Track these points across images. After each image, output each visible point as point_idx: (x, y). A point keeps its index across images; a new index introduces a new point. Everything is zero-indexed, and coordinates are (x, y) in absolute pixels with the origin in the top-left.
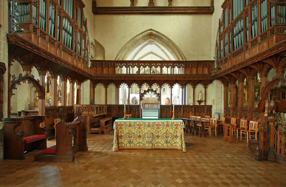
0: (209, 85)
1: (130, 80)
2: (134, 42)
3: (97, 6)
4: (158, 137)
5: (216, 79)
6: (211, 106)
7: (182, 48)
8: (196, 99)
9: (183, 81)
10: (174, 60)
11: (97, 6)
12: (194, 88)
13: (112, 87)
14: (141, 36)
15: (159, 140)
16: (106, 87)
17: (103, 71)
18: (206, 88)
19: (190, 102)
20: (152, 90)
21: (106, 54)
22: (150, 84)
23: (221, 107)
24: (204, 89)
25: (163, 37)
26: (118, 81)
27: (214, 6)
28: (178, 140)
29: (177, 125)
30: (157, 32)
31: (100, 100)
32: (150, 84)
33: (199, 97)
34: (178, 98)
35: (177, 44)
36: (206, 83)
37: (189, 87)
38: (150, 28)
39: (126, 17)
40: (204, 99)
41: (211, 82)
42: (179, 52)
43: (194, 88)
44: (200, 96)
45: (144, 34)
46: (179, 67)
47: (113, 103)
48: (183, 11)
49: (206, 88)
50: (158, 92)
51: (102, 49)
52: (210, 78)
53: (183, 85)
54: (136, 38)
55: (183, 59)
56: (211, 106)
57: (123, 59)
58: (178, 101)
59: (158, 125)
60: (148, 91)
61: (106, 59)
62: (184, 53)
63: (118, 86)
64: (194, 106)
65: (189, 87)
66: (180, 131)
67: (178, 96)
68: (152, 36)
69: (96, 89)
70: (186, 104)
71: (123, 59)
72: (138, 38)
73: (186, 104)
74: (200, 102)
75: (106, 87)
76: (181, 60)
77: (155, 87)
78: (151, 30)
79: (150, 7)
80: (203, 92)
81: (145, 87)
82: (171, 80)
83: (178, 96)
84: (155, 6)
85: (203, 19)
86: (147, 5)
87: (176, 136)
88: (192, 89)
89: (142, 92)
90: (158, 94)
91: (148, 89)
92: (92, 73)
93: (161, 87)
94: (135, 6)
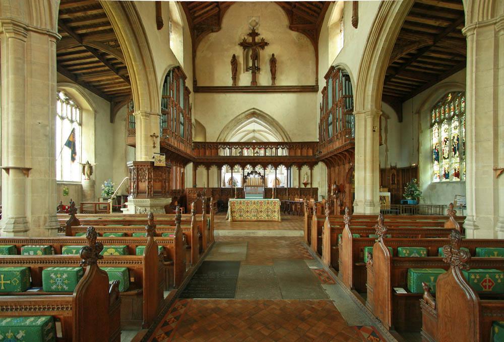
0: (315, 166)
1: (232, 162)
2: (237, 121)
3: (198, 85)
4: (261, 211)
5: (321, 161)
6: (317, 189)
7: (287, 128)
8: (302, 181)
9: (288, 162)
10: (277, 141)
11: (198, 85)
12: (300, 169)
13: (214, 169)
15: (262, 214)
16: (208, 169)
17: (205, 153)
18: (311, 169)
19: (295, 184)
20: (256, 172)
21: (207, 135)
22: (254, 165)
23: (326, 189)
24: (310, 171)
25: (267, 117)
26: (220, 163)
27: (319, 85)
28: (276, 214)
29: (275, 203)
31: (202, 183)
32: (254, 165)
33: (304, 179)
35: (281, 123)
36: (312, 165)
37: (294, 169)
39: (228, 95)
40: (310, 181)
41: (316, 163)
42: (284, 132)
43: (300, 169)
44: (305, 178)
45: (247, 113)
46: (283, 149)
47: (216, 186)
48: (287, 90)
49: (311, 169)
51: (203, 129)
52: (314, 160)
53: (288, 166)
54: (238, 118)
55: (287, 139)
56: (317, 189)
57: (224, 140)
58: (284, 184)
59: (261, 203)
60: (252, 173)
61: (208, 141)
62: (288, 133)
63: (220, 169)
64: (300, 189)
65: (294, 169)
66: (277, 208)
68: (255, 114)
69: (197, 171)
70: (292, 187)
71: (224, 140)
72: (240, 117)
73: (292, 187)
74: (306, 184)
75: (208, 169)
76: (286, 141)
77: (259, 169)
78: (254, 109)
79: (254, 87)
80: (309, 174)
81: (249, 168)
82: (275, 162)
84: (258, 85)
86: (250, 85)
87: (275, 211)
90: (262, 176)
91: (252, 172)
92: (194, 154)
93: (265, 169)
94: (237, 85)
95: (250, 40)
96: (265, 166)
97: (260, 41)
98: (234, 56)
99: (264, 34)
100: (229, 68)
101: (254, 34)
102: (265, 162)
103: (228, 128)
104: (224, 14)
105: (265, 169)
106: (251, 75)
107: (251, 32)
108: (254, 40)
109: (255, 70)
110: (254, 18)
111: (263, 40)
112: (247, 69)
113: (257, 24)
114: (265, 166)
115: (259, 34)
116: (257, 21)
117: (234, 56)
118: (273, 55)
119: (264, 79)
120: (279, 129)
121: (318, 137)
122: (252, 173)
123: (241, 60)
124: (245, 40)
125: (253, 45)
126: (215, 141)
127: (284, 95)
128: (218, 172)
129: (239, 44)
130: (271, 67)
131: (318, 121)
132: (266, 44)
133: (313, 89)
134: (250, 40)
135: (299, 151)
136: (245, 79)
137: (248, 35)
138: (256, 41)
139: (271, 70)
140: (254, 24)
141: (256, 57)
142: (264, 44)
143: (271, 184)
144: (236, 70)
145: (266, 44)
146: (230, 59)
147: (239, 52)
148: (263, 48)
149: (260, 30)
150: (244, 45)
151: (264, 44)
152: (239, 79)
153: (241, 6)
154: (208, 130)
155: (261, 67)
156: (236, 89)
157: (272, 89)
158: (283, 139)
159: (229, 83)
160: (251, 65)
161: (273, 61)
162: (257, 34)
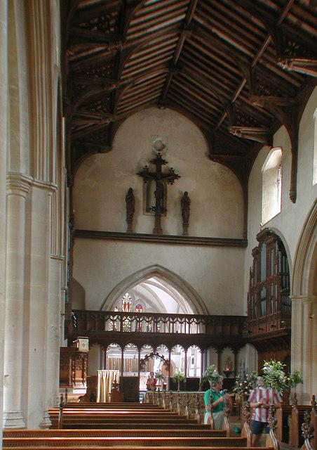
1: (123, 339)
2: (132, 280)
12: (220, 353)
14: (141, 275)
22: (155, 347)
30: (166, 269)
32: (155, 347)
34: (193, 363)
35: (195, 288)
36: (237, 347)
38: (154, 263)
43: (220, 353)
45: (148, 270)
48: (204, 243)
50: (166, 357)
55: (203, 310)
60: (152, 355)
61: (87, 309)
67: (193, 359)
76: (201, 313)
77: (163, 351)
80: (233, 359)
81: (148, 349)
82: (186, 341)
83: (193, 359)
85: (232, 253)
88: (217, 355)
89: (143, 357)
95: (153, 168)
96: (170, 348)
97: (167, 172)
98: (131, 191)
99: (173, 162)
100: (122, 206)
101: (159, 161)
102: (172, 341)
103: (117, 290)
104: (116, 130)
105: (170, 351)
106: (153, 219)
107: (154, 157)
108: (159, 169)
109: (159, 211)
110: (160, 139)
111: (172, 171)
112: (148, 210)
113: (164, 146)
114: (170, 348)
115: (167, 163)
116: (163, 142)
117: (131, 191)
118: (186, 193)
119: (172, 225)
120: (191, 295)
121: (246, 309)
122: (152, 355)
123: (140, 196)
124: (146, 169)
125: (158, 175)
126: (98, 310)
127: (200, 250)
128: (101, 351)
129: (138, 174)
130: (183, 210)
131: (246, 289)
132: (177, 177)
133: (241, 243)
134: (153, 168)
135: (220, 327)
136: (145, 224)
137: (151, 162)
138: (163, 170)
139: (183, 214)
140: (159, 146)
141: (161, 195)
142: (172, 176)
143: (178, 370)
144: (134, 211)
145: (177, 177)
146: (124, 194)
147: (137, 184)
148: (171, 181)
149: (167, 157)
150: (145, 174)
151: (172, 176)
152: (136, 222)
153: (141, 120)
154: (86, 292)
155: (167, 208)
156: (131, 236)
157: (183, 240)
158: (197, 309)
159: (123, 228)
160: (153, 203)
161: (185, 201)
162: (164, 162)
